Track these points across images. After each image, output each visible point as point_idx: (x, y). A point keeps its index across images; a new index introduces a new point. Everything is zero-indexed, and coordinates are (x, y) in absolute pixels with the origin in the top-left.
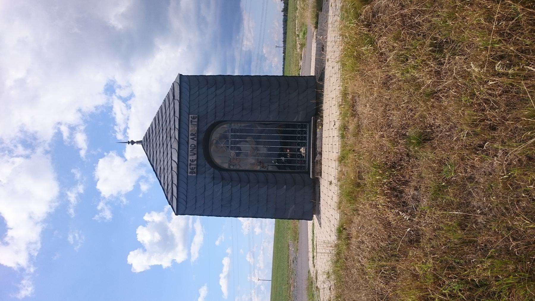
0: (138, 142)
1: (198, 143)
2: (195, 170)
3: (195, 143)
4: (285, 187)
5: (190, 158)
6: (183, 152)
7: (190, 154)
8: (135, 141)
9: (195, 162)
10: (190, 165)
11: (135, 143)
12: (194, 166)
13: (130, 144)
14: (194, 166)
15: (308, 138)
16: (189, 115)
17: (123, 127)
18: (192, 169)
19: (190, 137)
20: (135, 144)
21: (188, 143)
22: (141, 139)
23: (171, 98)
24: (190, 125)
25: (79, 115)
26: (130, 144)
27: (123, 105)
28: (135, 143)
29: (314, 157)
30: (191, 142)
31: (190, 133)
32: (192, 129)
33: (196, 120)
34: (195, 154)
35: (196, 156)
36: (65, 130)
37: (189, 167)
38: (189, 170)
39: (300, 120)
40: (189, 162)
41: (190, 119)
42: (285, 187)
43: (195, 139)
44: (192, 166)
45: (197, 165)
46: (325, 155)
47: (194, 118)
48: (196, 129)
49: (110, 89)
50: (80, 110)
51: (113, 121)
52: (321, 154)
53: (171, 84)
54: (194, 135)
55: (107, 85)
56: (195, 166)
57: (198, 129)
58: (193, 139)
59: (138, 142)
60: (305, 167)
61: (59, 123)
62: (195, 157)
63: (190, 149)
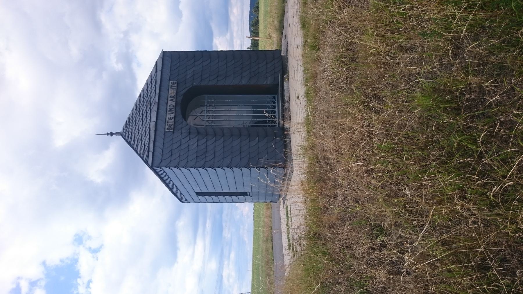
0: (117, 134)
1: (176, 104)
2: (172, 127)
3: (174, 103)
4: (257, 138)
5: (168, 116)
6: (162, 112)
7: (168, 113)
8: (114, 132)
9: (173, 120)
10: (168, 122)
11: (114, 134)
12: (171, 123)
13: (109, 136)
14: (171, 123)
15: (277, 107)
16: (170, 80)
17: (86, 281)
18: (170, 126)
19: (169, 99)
20: (114, 136)
21: (167, 104)
22: (120, 130)
23: (154, 80)
24: (170, 90)
25: (42, 268)
26: (109, 136)
27: (89, 255)
28: (114, 134)
29: (283, 106)
30: (170, 103)
31: (169, 96)
32: (172, 92)
33: (176, 85)
34: (173, 113)
35: (174, 114)
36: (24, 286)
37: (167, 124)
38: (167, 127)
39: (268, 83)
40: (167, 120)
41: (170, 84)
42: (257, 138)
43: (174, 100)
44: (169, 123)
45: (175, 122)
46: (293, 103)
47: (174, 84)
48: (175, 92)
49: (79, 240)
50: (44, 263)
51: (77, 275)
52: (289, 102)
53: (155, 63)
54: (173, 97)
55: (76, 235)
56: (173, 123)
57: (177, 92)
58: (171, 100)
59: (117, 134)
60: (275, 126)
61: (19, 278)
62: (173, 116)
63: (168, 109)
